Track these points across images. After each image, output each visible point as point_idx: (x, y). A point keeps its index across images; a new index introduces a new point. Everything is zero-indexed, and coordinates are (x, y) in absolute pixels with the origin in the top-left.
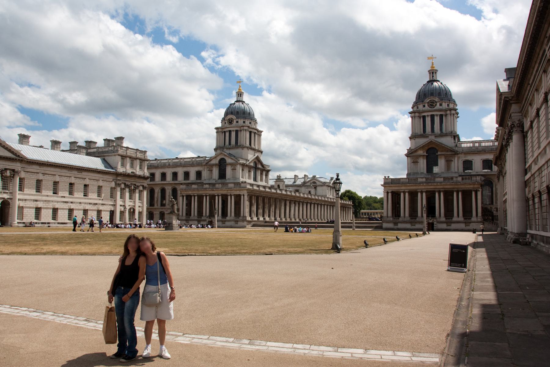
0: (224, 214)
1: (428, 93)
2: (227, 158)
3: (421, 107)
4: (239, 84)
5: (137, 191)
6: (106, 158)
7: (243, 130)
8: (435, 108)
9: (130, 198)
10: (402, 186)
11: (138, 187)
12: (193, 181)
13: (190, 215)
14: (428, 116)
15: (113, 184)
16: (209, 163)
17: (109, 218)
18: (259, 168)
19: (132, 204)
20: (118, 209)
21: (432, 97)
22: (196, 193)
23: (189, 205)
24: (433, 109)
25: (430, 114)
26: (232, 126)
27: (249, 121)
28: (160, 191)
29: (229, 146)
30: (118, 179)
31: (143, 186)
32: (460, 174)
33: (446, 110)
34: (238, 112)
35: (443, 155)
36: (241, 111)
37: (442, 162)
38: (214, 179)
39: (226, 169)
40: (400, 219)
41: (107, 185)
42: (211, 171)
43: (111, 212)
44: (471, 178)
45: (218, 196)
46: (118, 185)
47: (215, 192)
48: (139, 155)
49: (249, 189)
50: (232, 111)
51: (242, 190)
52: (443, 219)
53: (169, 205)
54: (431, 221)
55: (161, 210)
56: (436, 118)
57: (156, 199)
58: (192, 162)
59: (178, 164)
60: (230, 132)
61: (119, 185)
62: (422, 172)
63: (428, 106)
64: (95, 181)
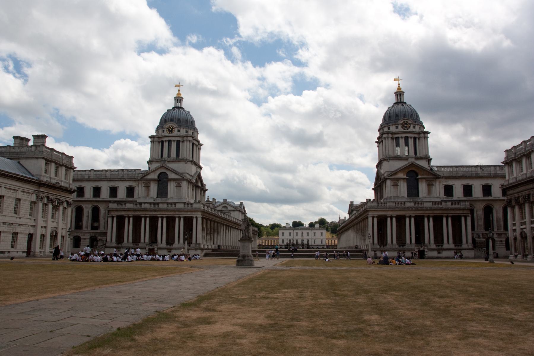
0: (170, 240)
1: (401, 114)
2: (168, 173)
3: (393, 129)
4: (177, 88)
6: (22, 162)
7: (187, 141)
8: (409, 130)
10: (388, 210)
11: (63, 202)
12: (123, 199)
13: (123, 241)
14: (402, 137)
15: (34, 198)
16: (146, 178)
17: (26, 244)
18: (199, 187)
19: (55, 225)
20: (39, 232)
21: (405, 118)
22: (131, 214)
24: (407, 131)
25: (404, 135)
26: (173, 134)
27: (192, 131)
29: (169, 159)
30: (41, 190)
31: (67, 202)
32: (442, 199)
33: (419, 133)
34: (179, 120)
35: (424, 178)
36: (183, 119)
37: (423, 187)
38: (152, 198)
39: (167, 186)
40: (388, 247)
42: (147, 187)
43: (30, 236)
44: (460, 203)
46: (39, 198)
47: (158, 214)
48: (64, 161)
49: (203, 212)
50: (173, 118)
51: (195, 211)
52: (434, 246)
53: (87, 227)
54: (421, 249)
55: (76, 234)
56: (410, 140)
58: (121, 175)
59: (102, 178)
60: (170, 142)
61: (42, 199)
62: (403, 196)
63: (402, 127)
64: (12, 191)
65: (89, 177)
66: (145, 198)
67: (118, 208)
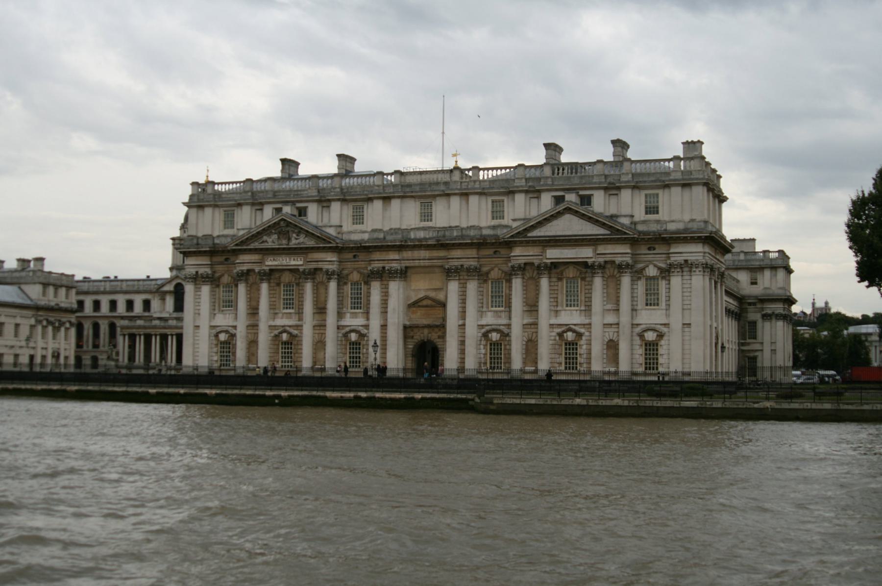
5: (63, 329)
6: (23, 287)
9: (54, 337)
11: (64, 323)
12: (138, 313)
13: (134, 361)
19: (57, 346)
22: (142, 331)
23: (132, 347)
28: (91, 327)
31: (70, 322)
38: (167, 312)
41: (26, 322)
42: (163, 299)
45: (172, 335)
46: (39, 322)
47: (168, 331)
48: (64, 282)
53: (104, 346)
57: (85, 339)
61: (40, 322)
65: (105, 289)
66: (161, 312)
67: (130, 324)
